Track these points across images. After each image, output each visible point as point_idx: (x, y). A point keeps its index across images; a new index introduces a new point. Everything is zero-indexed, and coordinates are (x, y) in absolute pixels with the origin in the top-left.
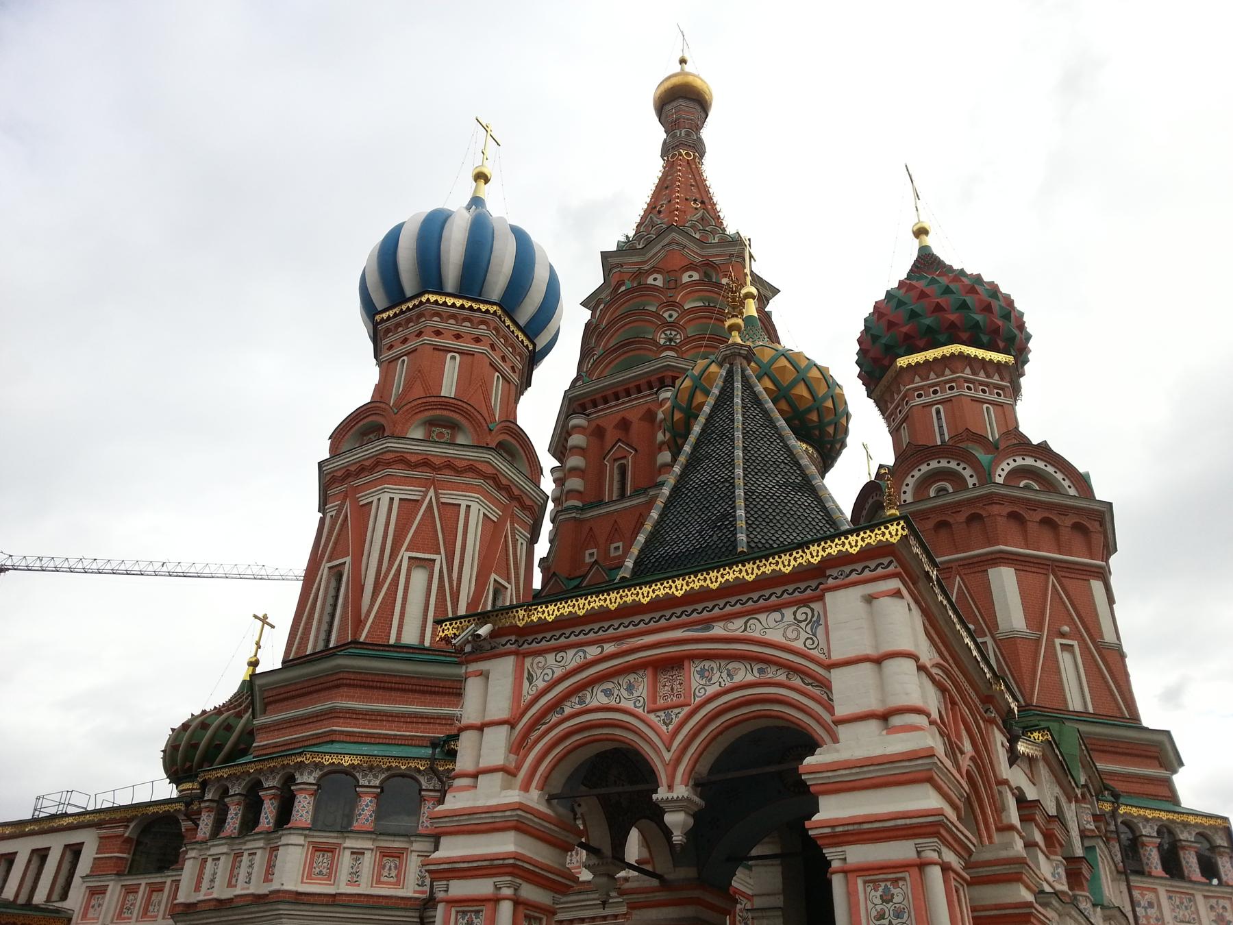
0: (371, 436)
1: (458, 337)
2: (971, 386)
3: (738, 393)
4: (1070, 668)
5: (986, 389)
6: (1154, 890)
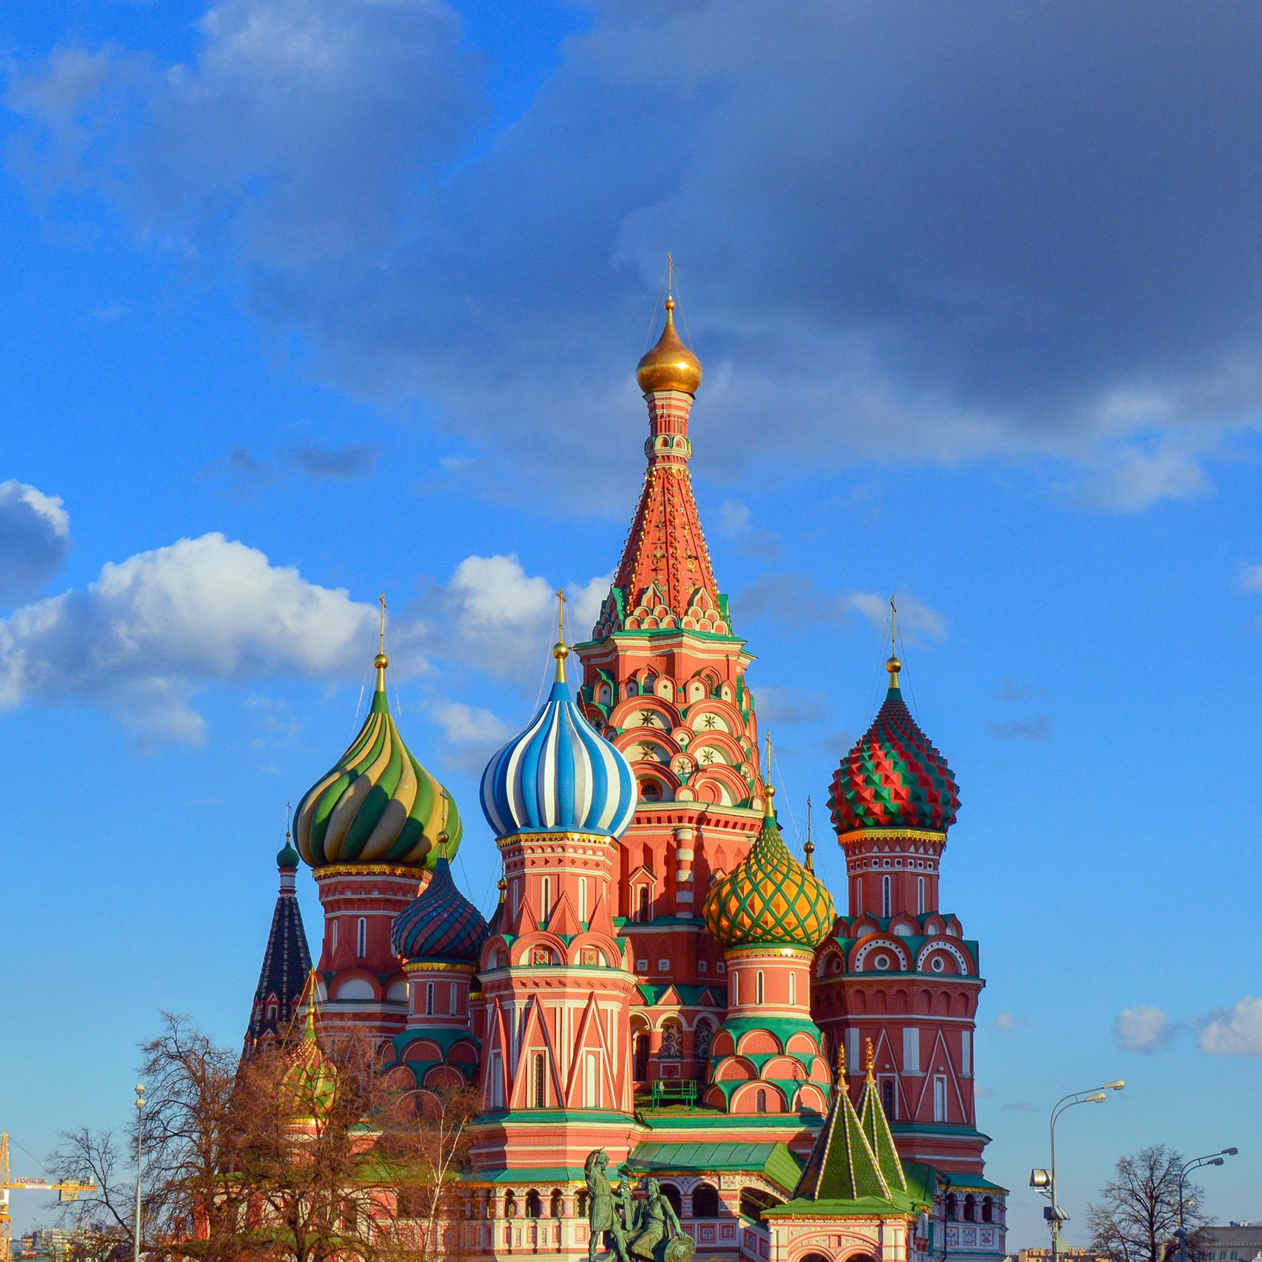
0: (542, 952)
2: (913, 861)
3: (846, 1115)
4: (939, 1092)
5: (922, 862)
6: (958, 1228)
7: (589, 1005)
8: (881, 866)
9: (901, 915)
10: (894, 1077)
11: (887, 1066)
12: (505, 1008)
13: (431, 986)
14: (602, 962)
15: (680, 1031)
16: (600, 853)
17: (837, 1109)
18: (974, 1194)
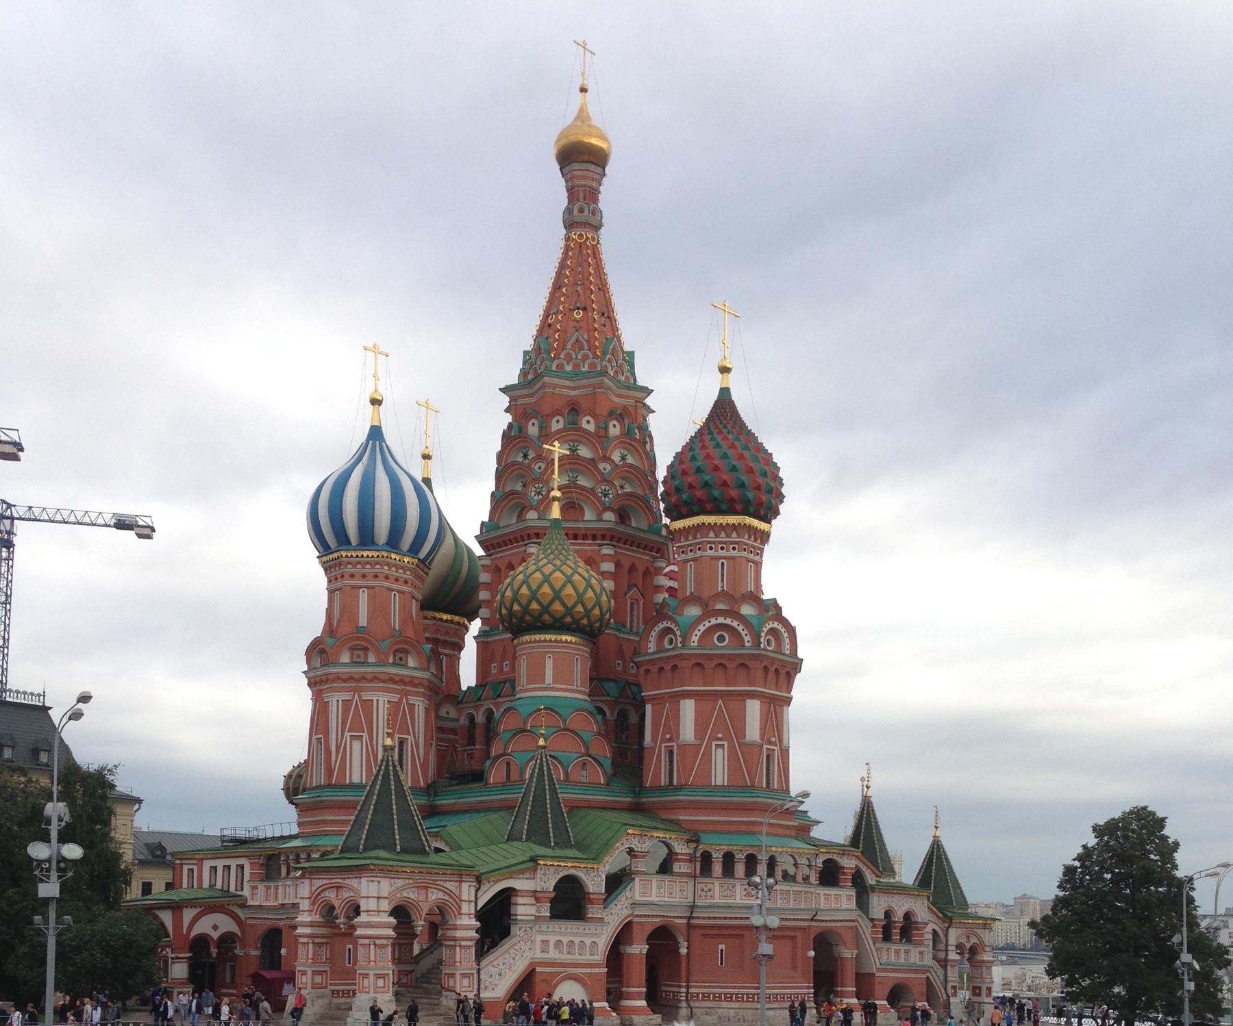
1: (364, 576)
9: (695, 599)
11: (668, 736)
14: (372, 658)
16: (378, 566)
18: (733, 852)
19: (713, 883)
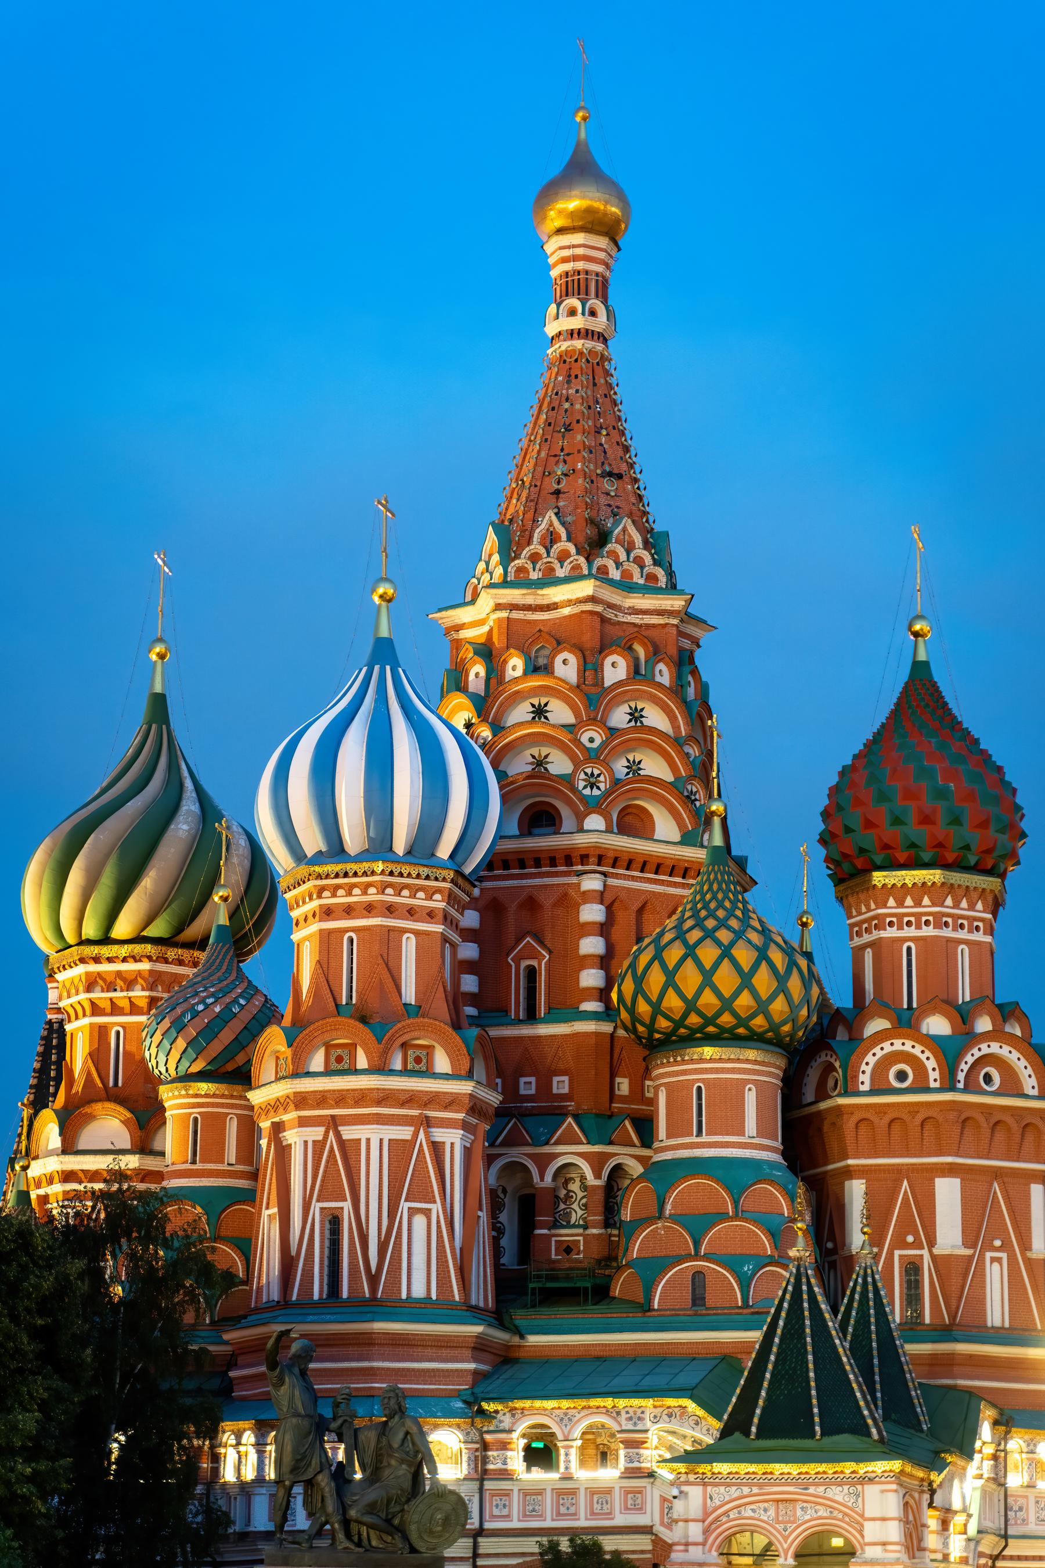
0: (339, 1051)
1: (411, 912)
3: (805, 1296)
6: (1026, 1497)
7: (416, 1135)
8: (900, 928)
10: (922, 1256)
11: (910, 1239)
12: (284, 1143)
13: (196, 1119)
15: (584, 1187)
16: (438, 897)
17: (790, 1288)
19: (1026, 1497)
